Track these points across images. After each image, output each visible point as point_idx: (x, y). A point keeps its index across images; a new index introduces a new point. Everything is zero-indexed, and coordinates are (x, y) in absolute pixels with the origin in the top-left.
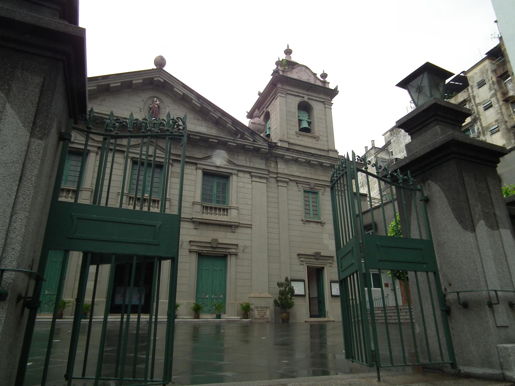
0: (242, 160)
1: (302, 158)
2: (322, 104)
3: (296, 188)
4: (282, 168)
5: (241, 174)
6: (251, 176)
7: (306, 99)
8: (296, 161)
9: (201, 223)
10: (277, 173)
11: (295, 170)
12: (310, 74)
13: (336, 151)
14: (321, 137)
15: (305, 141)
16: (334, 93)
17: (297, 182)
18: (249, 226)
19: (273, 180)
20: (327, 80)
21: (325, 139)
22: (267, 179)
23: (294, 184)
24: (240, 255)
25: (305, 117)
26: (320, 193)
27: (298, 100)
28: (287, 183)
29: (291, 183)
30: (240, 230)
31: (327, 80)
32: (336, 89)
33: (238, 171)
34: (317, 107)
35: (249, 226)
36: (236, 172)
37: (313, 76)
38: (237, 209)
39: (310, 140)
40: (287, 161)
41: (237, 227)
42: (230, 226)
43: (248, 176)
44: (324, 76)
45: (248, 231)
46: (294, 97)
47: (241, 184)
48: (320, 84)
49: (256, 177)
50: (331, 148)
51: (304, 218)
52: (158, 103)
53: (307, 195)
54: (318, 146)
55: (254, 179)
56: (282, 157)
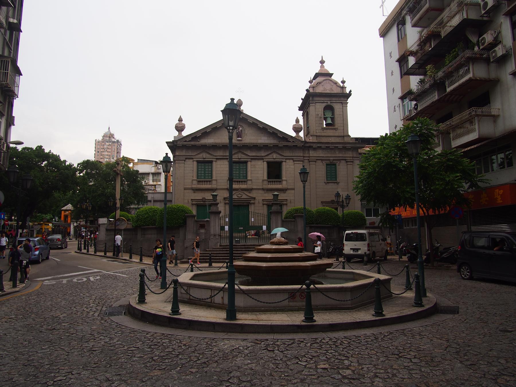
0: (287, 153)
1: (323, 146)
2: (341, 104)
3: (321, 164)
4: (312, 153)
5: (287, 161)
6: (294, 161)
7: (329, 103)
8: (320, 148)
9: (267, 190)
10: (309, 157)
11: (320, 154)
12: (333, 84)
13: (349, 136)
14: (339, 128)
15: (330, 133)
16: (349, 95)
17: (322, 160)
18: (293, 189)
19: (306, 161)
20: (345, 85)
21: (342, 128)
22: (303, 161)
23: (320, 161)
24: (289, 204)
25: (329, 114)
26: (337, 164)
27: (325, 105)
28: (315, 162)
29: (318, 161)
30: (288, 192)
31: (345, 85)
32: (350, 91)
33: (286, 159)
34: (337, 107)
35: (293, 189)
36: (285, 160)
37: (335, 86)
38: (286, 181)
39: (332, 131)
40: (315, 149)
41: (286, 190)
42: (283, 190)
43: (292, 161)
44: (343, 82)
45: (293, 191)
46: (321, 104)
47: (288, 166)
48: (338, 91)
49: (296, 161)
50: (345, 134)
51: (326, 181)
52: (241, 129)
53: (329, 166)
54: (337, 134)
55: (295, 162)
56: (310, 147)
